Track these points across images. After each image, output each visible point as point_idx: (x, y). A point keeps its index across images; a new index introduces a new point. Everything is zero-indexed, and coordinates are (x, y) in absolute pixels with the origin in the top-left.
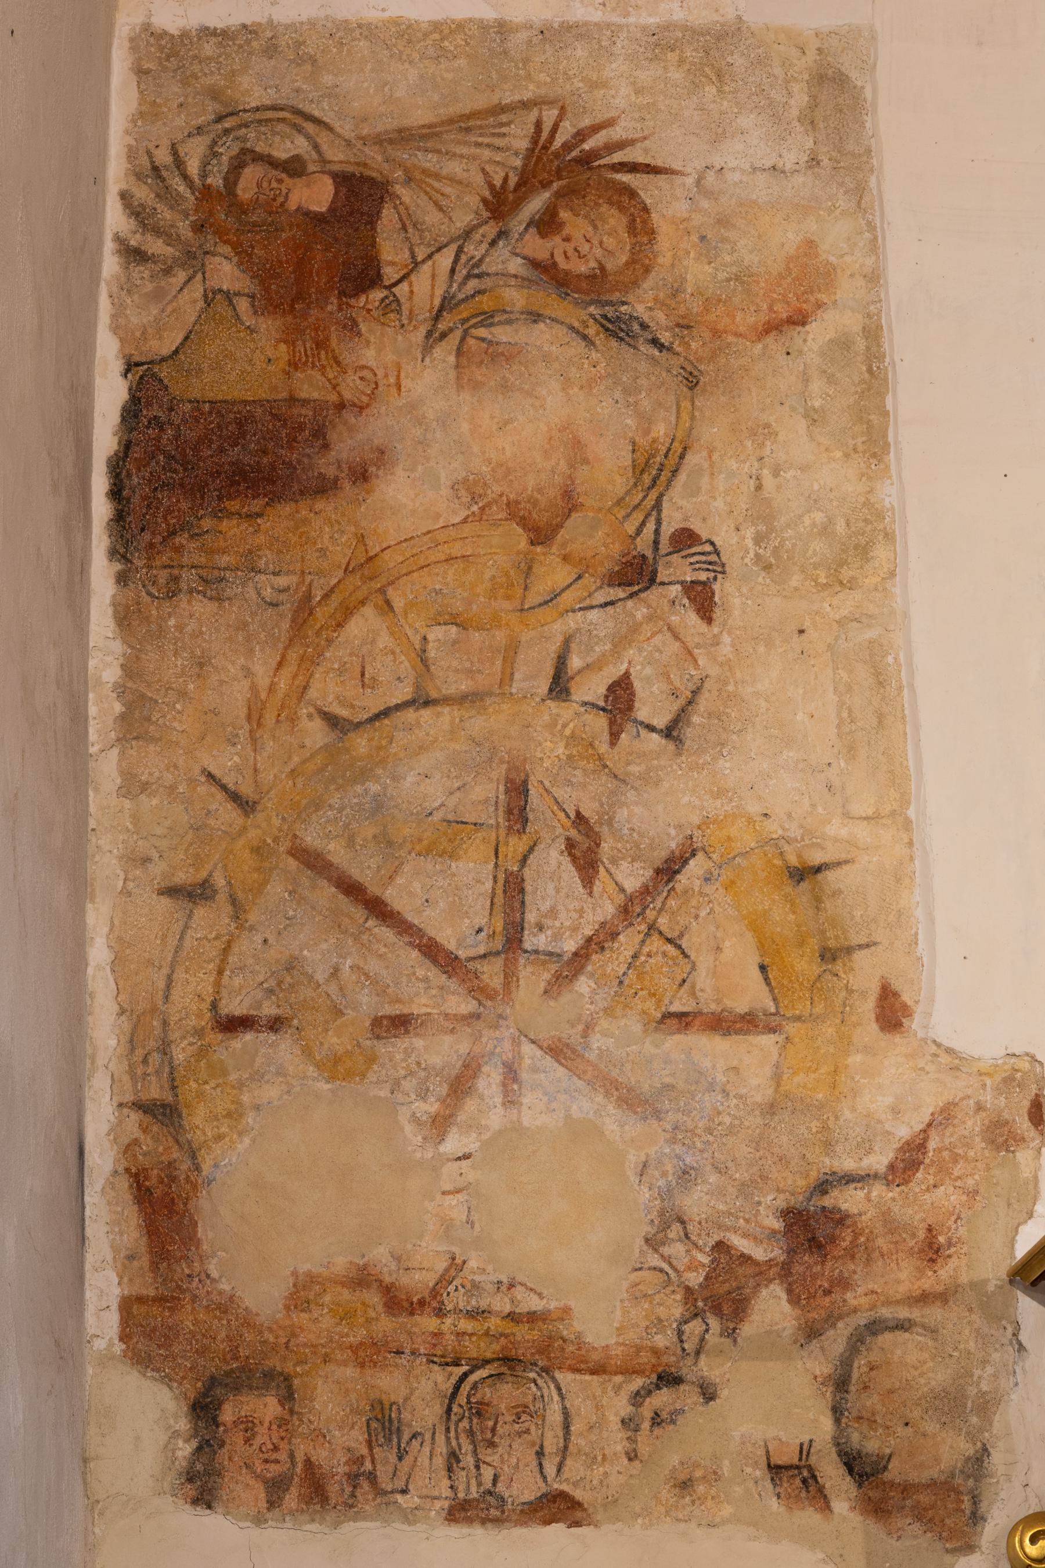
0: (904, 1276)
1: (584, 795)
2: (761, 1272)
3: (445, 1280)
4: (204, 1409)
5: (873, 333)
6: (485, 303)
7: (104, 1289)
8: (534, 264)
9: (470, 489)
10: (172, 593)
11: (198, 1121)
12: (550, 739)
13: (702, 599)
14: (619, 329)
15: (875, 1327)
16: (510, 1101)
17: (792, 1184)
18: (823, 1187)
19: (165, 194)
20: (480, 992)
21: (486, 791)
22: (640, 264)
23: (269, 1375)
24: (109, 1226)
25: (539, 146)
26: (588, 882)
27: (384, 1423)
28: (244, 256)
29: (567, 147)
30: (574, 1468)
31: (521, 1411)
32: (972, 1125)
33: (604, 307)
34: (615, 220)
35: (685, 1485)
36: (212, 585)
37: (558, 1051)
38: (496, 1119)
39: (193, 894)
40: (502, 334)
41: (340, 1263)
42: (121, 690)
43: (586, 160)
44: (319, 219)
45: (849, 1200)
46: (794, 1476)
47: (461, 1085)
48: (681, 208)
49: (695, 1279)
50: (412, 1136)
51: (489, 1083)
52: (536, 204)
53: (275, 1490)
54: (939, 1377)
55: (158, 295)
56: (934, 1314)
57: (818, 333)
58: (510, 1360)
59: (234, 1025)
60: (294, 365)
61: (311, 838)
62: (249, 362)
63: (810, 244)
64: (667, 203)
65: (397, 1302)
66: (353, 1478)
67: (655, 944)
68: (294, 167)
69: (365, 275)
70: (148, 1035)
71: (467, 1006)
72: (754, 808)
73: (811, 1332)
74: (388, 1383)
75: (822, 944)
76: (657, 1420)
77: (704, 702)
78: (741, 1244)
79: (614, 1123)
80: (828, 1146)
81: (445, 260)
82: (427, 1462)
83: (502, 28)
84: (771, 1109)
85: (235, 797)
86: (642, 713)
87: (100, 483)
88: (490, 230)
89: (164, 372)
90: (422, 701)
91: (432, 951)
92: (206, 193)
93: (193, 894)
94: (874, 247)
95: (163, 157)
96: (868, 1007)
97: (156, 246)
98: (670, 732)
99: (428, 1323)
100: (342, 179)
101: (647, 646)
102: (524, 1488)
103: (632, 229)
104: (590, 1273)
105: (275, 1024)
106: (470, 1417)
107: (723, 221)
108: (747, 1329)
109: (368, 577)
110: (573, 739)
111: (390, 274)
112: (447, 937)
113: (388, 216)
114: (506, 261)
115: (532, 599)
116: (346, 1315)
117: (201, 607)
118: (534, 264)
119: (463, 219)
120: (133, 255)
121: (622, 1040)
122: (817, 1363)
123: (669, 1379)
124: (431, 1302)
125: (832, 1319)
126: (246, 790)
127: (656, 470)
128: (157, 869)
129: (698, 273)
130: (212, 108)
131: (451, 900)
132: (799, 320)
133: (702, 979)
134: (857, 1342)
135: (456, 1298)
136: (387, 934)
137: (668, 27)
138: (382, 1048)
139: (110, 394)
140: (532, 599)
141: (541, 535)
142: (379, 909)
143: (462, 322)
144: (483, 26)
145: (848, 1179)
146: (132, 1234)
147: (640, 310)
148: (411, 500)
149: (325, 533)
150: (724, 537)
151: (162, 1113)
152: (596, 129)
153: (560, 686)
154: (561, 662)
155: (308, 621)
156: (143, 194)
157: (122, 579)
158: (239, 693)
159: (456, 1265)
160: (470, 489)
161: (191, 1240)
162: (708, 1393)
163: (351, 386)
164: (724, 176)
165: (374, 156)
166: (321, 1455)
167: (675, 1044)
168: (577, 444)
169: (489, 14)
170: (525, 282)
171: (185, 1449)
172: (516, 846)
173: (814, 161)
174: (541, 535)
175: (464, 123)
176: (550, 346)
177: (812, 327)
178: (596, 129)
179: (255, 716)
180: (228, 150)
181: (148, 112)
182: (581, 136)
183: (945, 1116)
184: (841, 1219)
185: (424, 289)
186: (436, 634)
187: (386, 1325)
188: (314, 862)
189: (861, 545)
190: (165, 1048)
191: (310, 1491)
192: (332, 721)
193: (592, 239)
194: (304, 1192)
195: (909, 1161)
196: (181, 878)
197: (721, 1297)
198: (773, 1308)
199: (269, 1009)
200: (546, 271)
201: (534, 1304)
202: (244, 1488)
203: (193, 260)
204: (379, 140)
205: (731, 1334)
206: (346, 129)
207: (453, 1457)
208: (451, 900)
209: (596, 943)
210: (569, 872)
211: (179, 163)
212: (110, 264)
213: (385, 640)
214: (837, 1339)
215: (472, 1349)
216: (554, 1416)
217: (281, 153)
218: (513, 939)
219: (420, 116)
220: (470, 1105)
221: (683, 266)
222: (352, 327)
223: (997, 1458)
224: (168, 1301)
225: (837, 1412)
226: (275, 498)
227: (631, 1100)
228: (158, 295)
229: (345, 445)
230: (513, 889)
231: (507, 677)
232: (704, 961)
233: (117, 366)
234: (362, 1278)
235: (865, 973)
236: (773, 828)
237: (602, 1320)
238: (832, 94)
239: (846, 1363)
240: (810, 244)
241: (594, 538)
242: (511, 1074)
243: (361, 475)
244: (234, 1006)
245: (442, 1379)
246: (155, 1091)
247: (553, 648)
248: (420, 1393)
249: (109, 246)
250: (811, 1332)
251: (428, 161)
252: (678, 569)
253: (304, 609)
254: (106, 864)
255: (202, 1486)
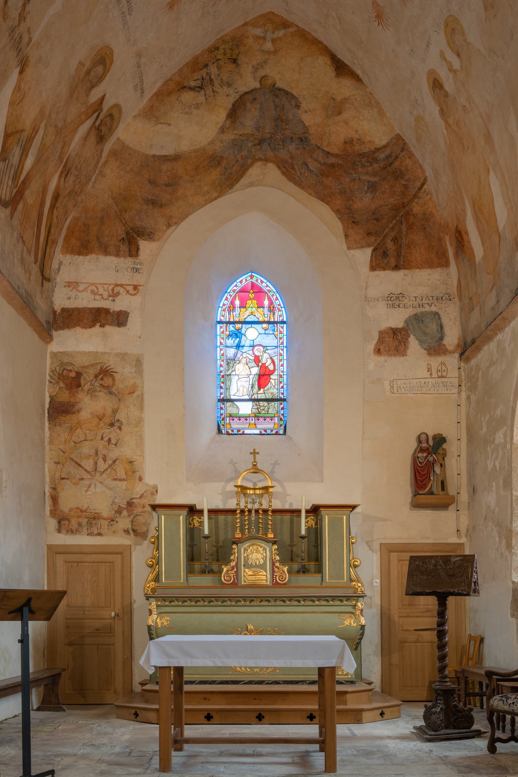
0: (140, 509)
1: (105, 452)
2: (124, 509)
3: (87, 509)
4: (59, 522)
5: (142, 394)
6: (94, 389)
7: (48, 509)
8: (100, 384)
9: (92, 413)
10: (55, 426)
11: (59, 490)
12: (101, 445)
13: (120, 428)
14: (111, 393)
15: (137, 515)
16: (95, 488)
17: (128, 499)
18: (131, 499)
19: (54, 374)
20: (92, 475)
21: (93, 451)
22: (114, 385)
23: (67, 519)
24: (48, 502)
25: (101, 369)
26: (105, 463)
27: (80, 524)
28: (64, 382)
29: (105, 369)
30: (102, 530)
31: (96, 524)
32: (149, 492)
33: (108, 390)
34: (111, 379)
35: (114, 532)
36: (60, 425)
37: (101, 483)
38: (93, 490)
39: (58, 463)
40: (96, 393)
41: (75, 506)
42: (49, 438)
43: (107, 371)
44: (73, 378)
45: (134, 501)
46: (127, 532)
47: (89, 486)
48: (119, 377)
49: (116, 509)
50: (83, 492)
51: (93, 486)
52: (101, 377)
53: (67, 531)
54: (144, 521)
55: (53, 387)
56: (143, 514)
57: (135, 394)
58: (94, 518)
59: (63, 479)
60: (70, 397)
61: (72, 457)
62: (65, 396)
63: (135, 383)
64: (117, 377)
65: (82, 511)
66: (76, 530)
67: (113, 470)
68: (70, 371)
69: (79, 385)
70: (52, 480)
71: (90, 477)
72: (125, 454)
73: (129, 516)
74: (80, 520)
75: (133, 470)
76: (111, 525)
77: (120, 441)
78: (122, 505)
79: (107, 491)
80: (132, 494)
81: (89, 384)
82: (85, 529)
83: (97, 352)
84: (126, 490)
85: (63, 451)
86: (112, 442)
87: (46, 412)
88: (95, 380)
89: (54, 398)
90: (85, 440)
91: (86, 470)
92: (59, 374)
93: (58, 463)
94: (143, 383)
95: (54, 369)
96: (138, 478)
97: (53, 381)
98: (115, 445)
99: (85, 513)
100: (77, 373)
101: (113, 434)
102: (96, 532)
103: (113, 380)
104: (103, 508)
105: (68, 479)
106: (90, 524)
107: (124, 379)
108: (122, 515)
109: (79, 424)
110: (104, 445)
111: (82, 385)
112: (88, 469)
113: (82, 377)
114: (97, 384)
115: (99, 427)
116: (76, 512)
117: (59, 428)
118: (100, 384)
119: (92, 378)
120: (50, 382)
121: (109, 482)
122: (130, 519)
123: (113, 520)
124: (86, 511)
125: (132, 514)
126: (64, 451)
127: (115, 411)
128: (53, 460)
129: (121, 386)
130: (60, 363)
131: (88, 464)
132: (133, 392)
133: (118, 475)
134: (134, 517)
135: (88, 511)
136: (81, 468)
137: (118, 353)
138: (80, 482)
139: (47, 400)
140: (99, 427)
141: (100, 420)
142: (80, 465)
143: (91, 392)
144: (95, 352)
145: (134, 498)
146: (51, 503)
147: (113, 391)
148: (85, 415)
149: (74, 418)
150: (123, 420)
151: (54, 489)
152: (108, 366)
153: (102, 439)
154: (102, 436)
155: (72, 430)
156: (51, 374)
157: (49, 424)
158: (63, 438)
159: (88, 507)
160: (92, 413)
161: (58, 503)
162: (117, 522)
163: (77, 400)
164: (124, 372)
165: (80, 369)
166: (73, 528)
167: (115, 482)
168: (105, 408)
169: (95, 350)
170: (99, 387)
171: (57, 527)
172: (96, 458)
173: (136, 372)
174: (100, 420)
175: (92, 365)
176: (102, 394)
177: (135, 393)
178: (108, 366)
179: (65, 441)
180: (62, 368)
181: (52, 363)
182: (107, 367)
183: (146, 491)
184: (133, 503)
185: (86, 387)
186: (87, 432)
187: (80, 513)
188: (72, 459)
189: (140, 422)
190: (54, 481)
191: (72, 532)
192: (75, 442)
193: (108, 381)
194: (71, 498)
195: (142, 496)
196: (56, 461)
197: (119, 511)
198: (125, 513)
199: (67, 477)
200: (102, 385)
201: (97, 512)
202: (64, 532)
203: (58, 383)
204: (81, 367)
205: (120, 515)
206: (77, 366)
207: (88, 528)
208: (88, 464)
209: (106, 470)
210: (103, 462)
211: (56, 370)
212: (47, 383)
213: (81, 432)
214: (132, 517)
215: (90, 517)
216: (99, 524)
217: (69, 369)
218: (96, 470)
219: (86, 364)
220: (90, 489)
221: (119, 385)
222: (77, 392)
223: (150, 530)
224: (55, 510)
225: (132, 525)
226: (68, 414)
227: (109, 489)
228: (53, 387)
229: (77, 407)
230: (96, 463)
231: (96, 437)
232: (118, 472)
233: (48, 397)
234: (77, 508)
235: (137, 474)
236: (127, 457)
237: (105, 514)
238: (138, 362)
239: (133, 519)
240: (135, 383)
241: (107, 420)
242: (95, 485)
243: (78, 411)
244: (63, 476)
245: (87, 520)
246: (53, 486)
247: (101, 434)
248: (84, 521)
249: (47, 381)
250: (129, 516)
251: (87, 370)
252: (117, 424)
253: (71, 428)
254: (47, 459)
255: (59, 531)
